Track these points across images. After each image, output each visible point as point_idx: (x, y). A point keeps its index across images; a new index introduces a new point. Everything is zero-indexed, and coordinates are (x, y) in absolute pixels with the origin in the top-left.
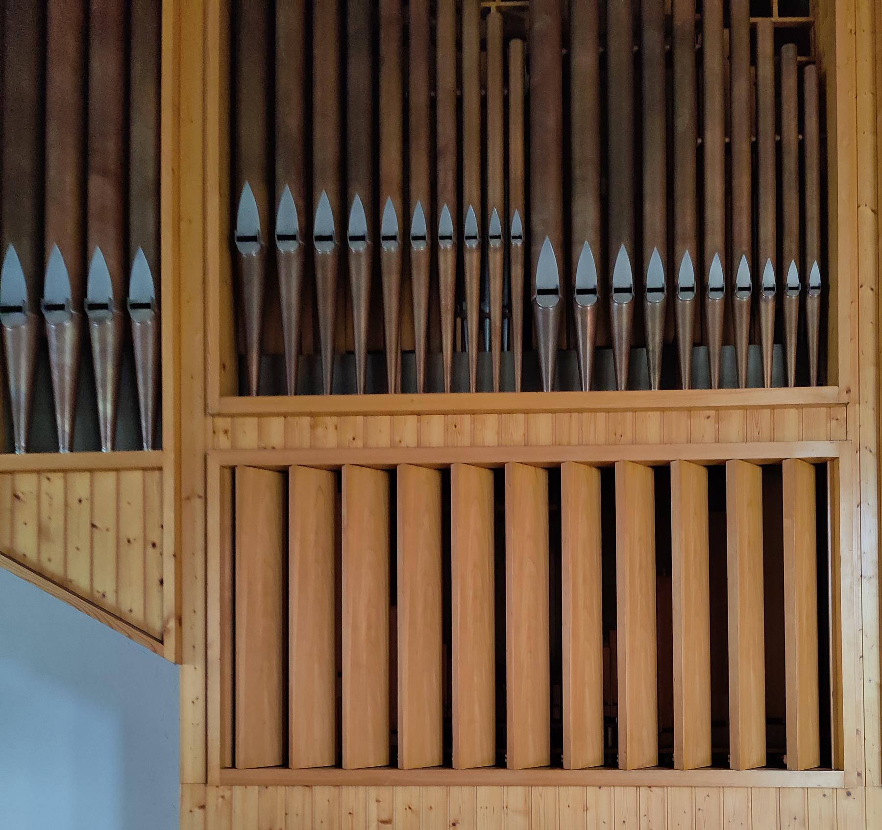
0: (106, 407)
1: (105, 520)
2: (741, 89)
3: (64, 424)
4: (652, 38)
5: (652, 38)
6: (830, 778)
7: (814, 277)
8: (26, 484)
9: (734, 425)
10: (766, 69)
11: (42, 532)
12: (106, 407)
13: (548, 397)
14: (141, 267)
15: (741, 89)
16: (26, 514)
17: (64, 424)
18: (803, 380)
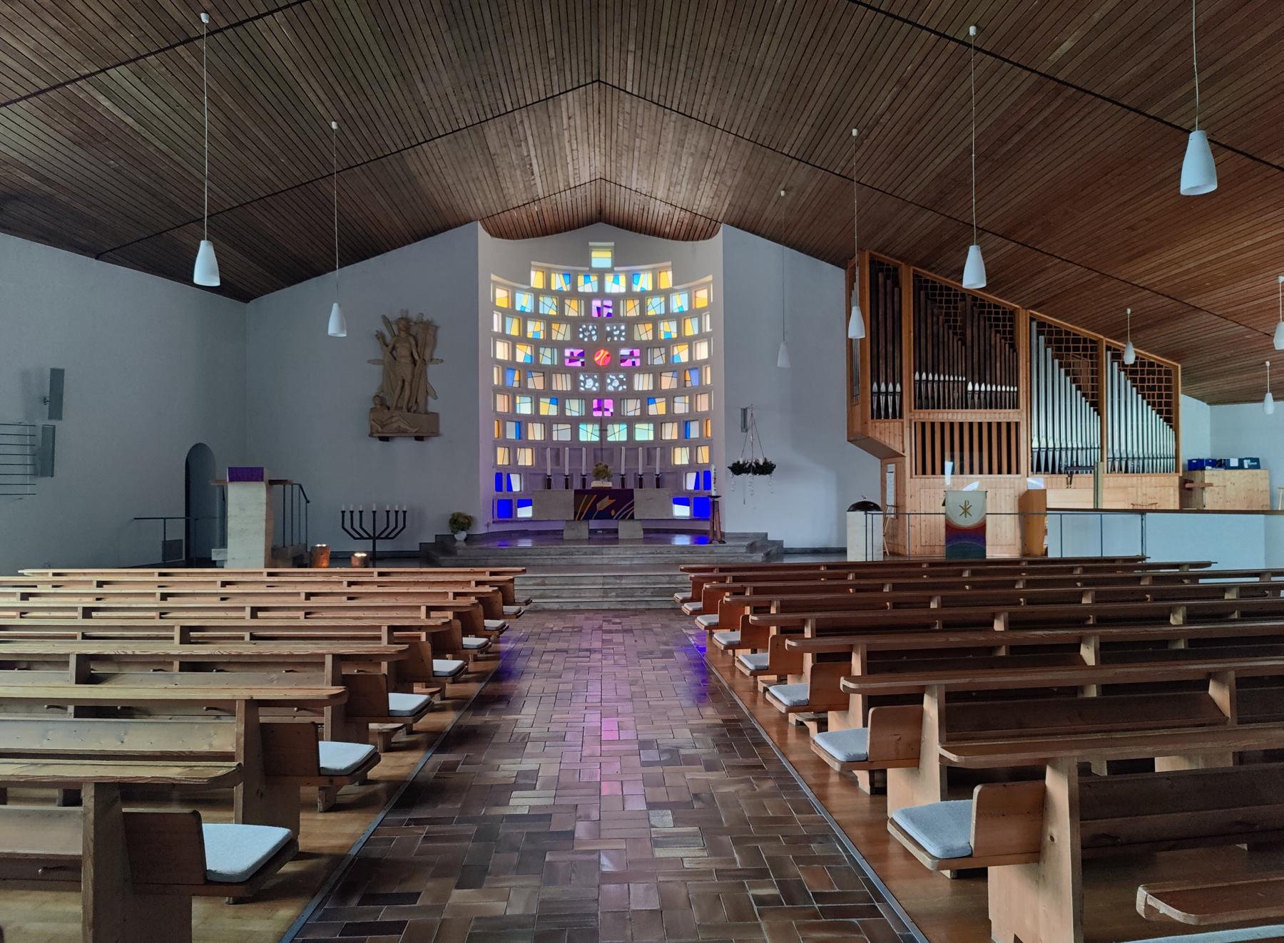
0: (890, 410)
1: (892, 431)
2: (1003, 356)
3: (883, 413)
4: (988, 348)
5: (988, 348)
6: (1018, 476)
7: (1016, 389)
8: (877, 424)
9: (1002, 415)
10: (1007, 353)
11: (880, 433)
12: (890, 410)
13: (969, 410)
14: (898, 387)
15: (1003, 356)
16: (878, 429)
17: (883, 413)
18: (1013, 408)
